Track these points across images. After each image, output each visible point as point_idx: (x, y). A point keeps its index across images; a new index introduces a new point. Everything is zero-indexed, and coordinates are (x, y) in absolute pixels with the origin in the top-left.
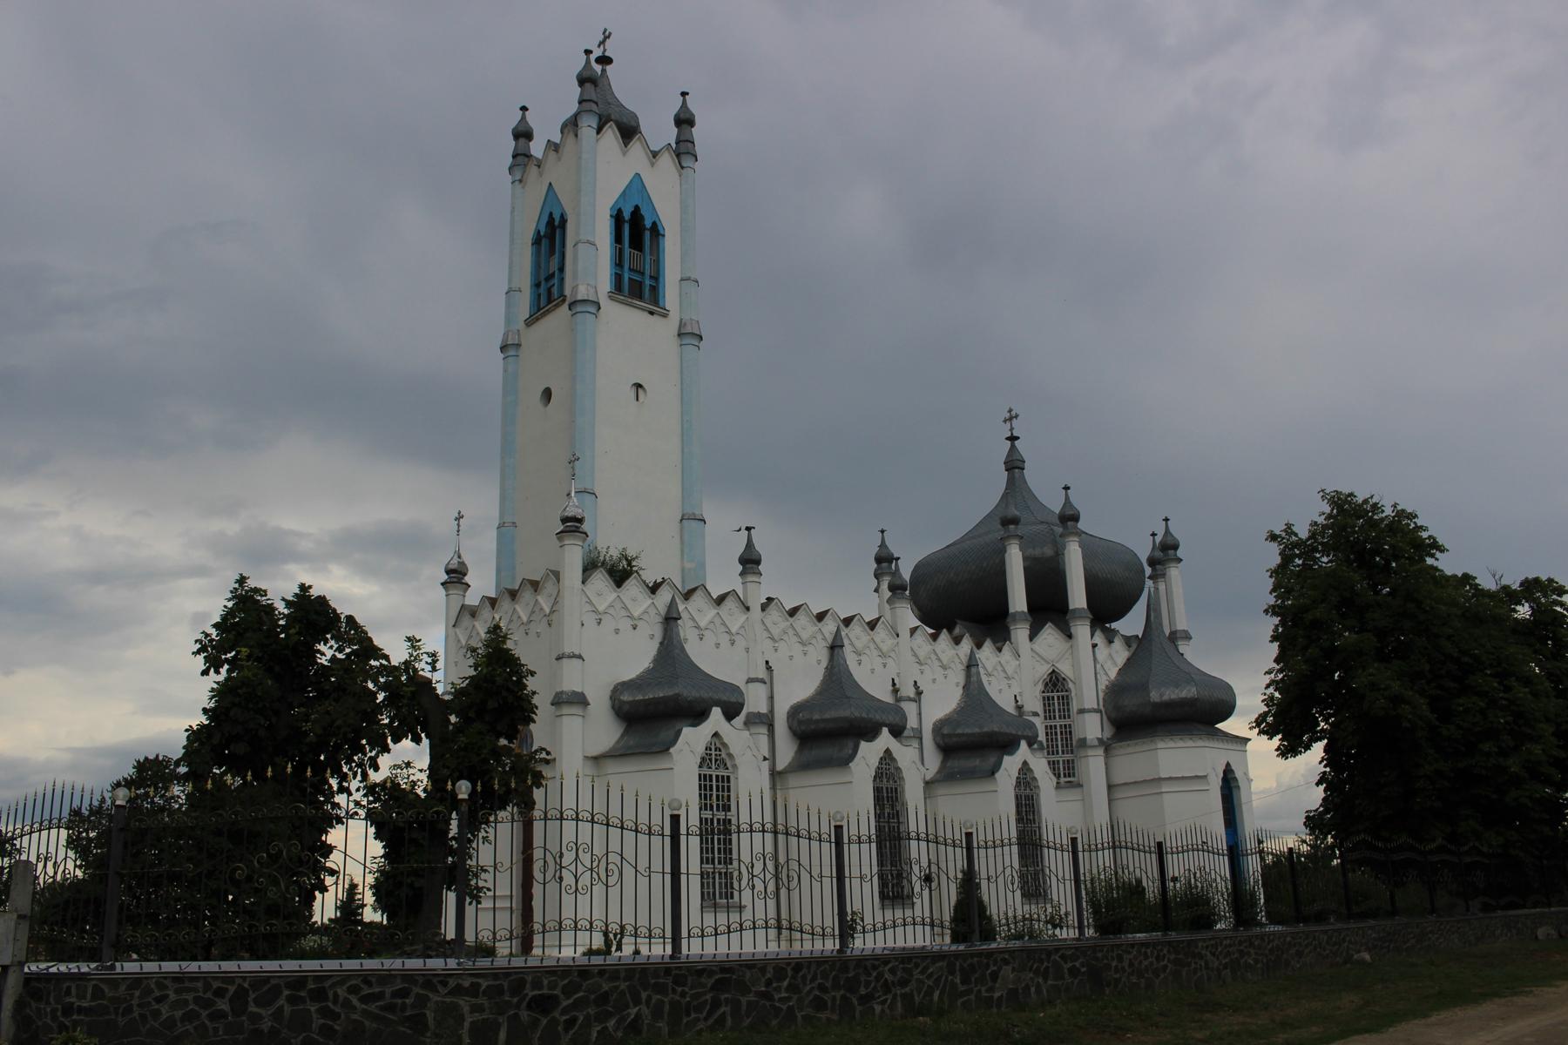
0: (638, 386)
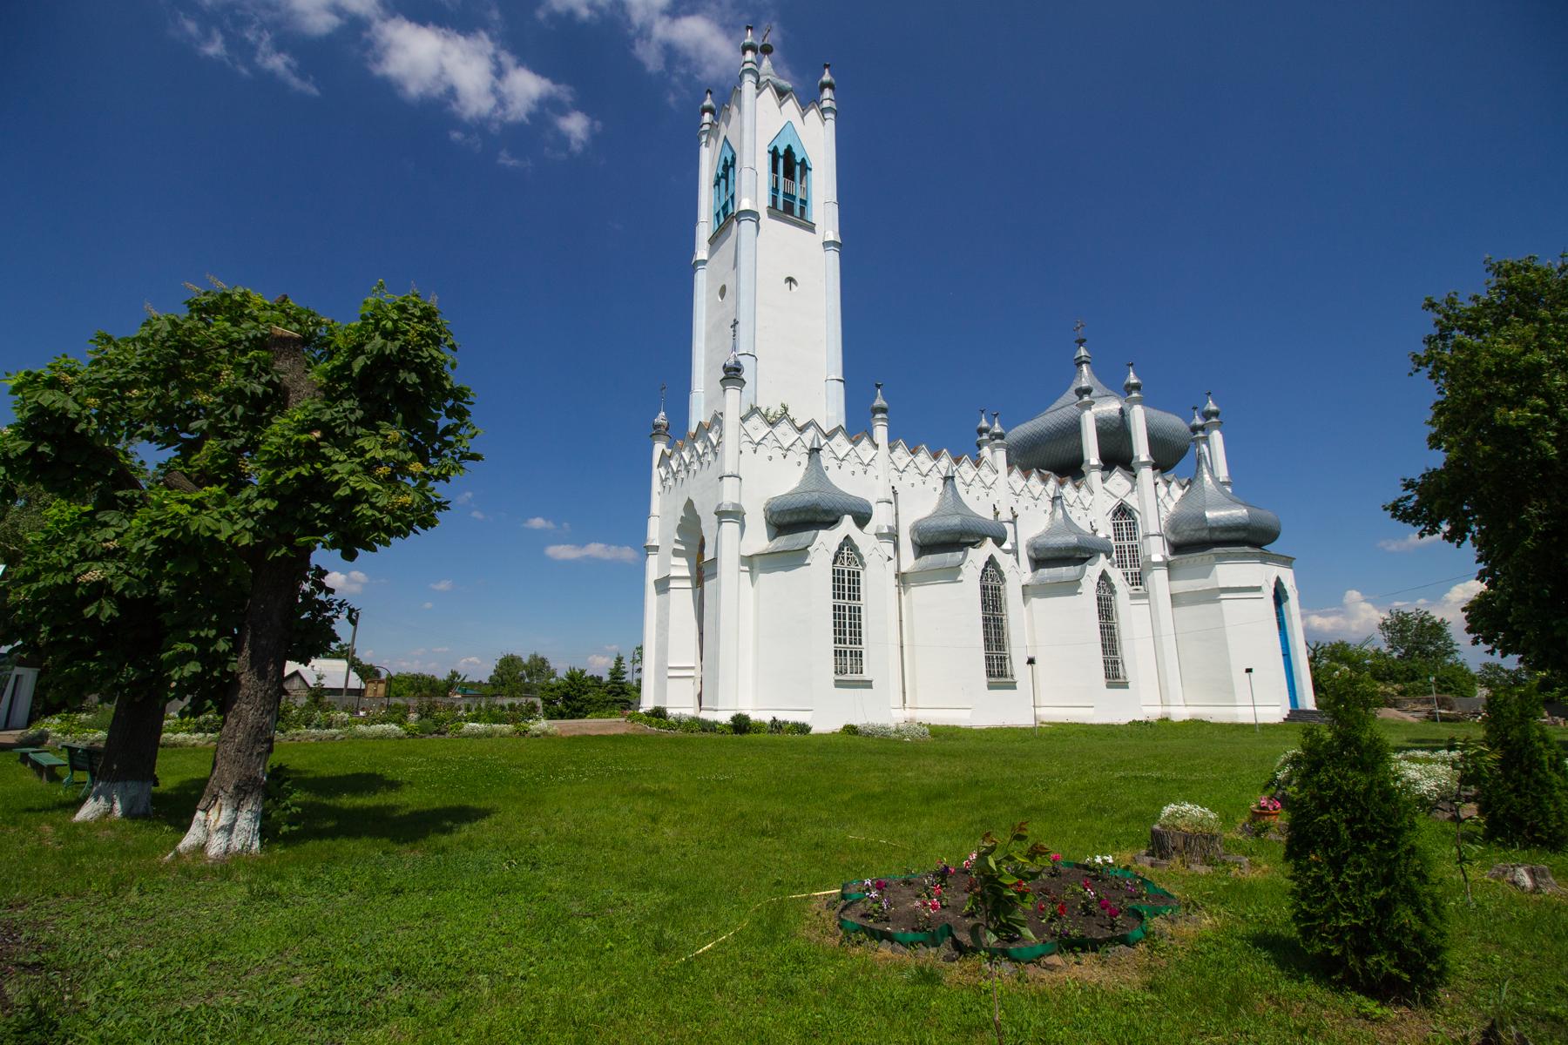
0: (790, 280)
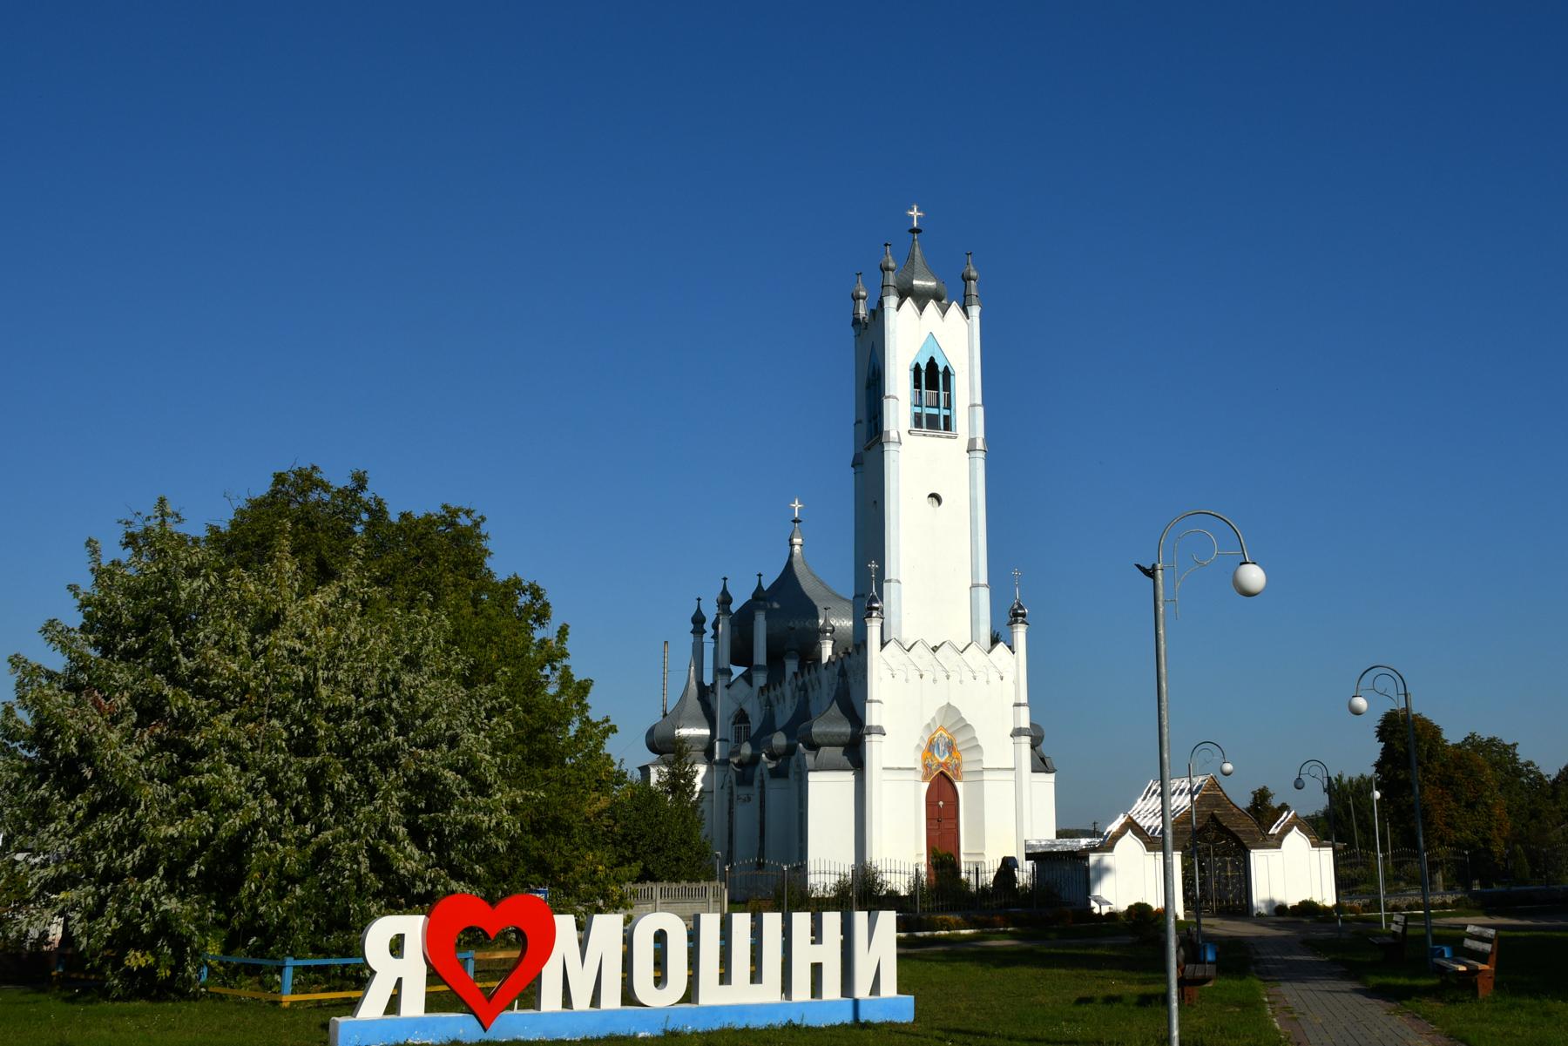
0: (936, 497)
